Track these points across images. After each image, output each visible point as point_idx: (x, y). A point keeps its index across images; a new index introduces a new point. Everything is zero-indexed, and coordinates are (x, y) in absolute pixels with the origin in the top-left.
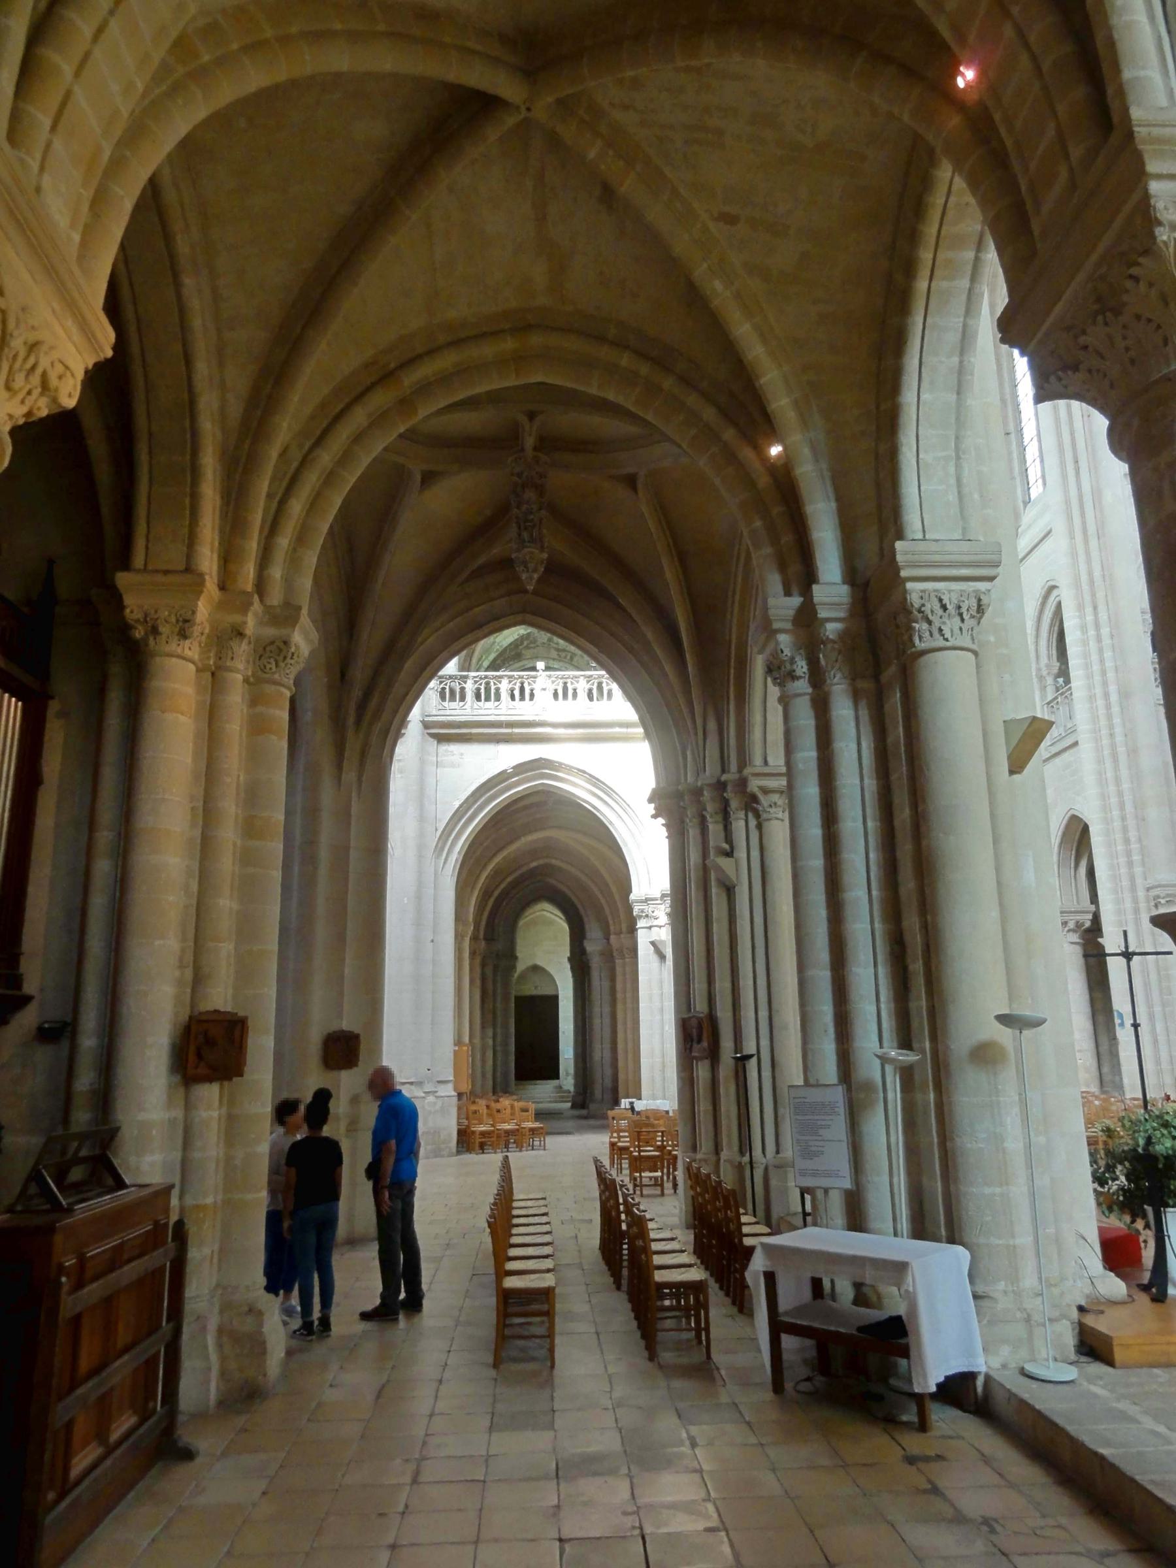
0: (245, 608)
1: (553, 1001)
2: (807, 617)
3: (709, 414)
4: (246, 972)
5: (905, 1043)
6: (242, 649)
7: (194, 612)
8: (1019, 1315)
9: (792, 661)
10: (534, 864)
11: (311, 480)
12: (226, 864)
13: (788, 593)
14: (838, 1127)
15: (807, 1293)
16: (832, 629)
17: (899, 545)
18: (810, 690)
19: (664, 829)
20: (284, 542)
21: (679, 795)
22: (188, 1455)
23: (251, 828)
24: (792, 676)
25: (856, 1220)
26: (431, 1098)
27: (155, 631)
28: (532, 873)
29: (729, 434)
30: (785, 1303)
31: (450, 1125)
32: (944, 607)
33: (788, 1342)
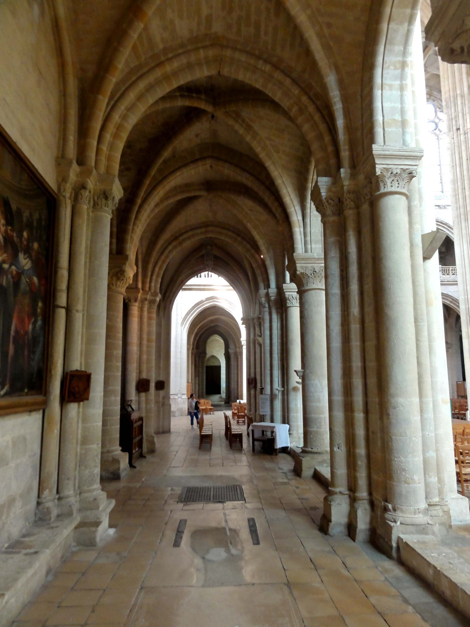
0: (147, 294)
1: (219, 368)
2: (267, 295)
3: (248, 246)
4: (149, 370)
5: (283, 387)
6: (147, 303)
7: (138, 297)
8: (297, 437)
9: (265, 303)
10: (212, 325)
11: (160, 263)
12: (145, 348)
13: (265, 289)
14: (268, 403)
15: (261, 435)
16: (273, 298)
17: (284, 285)
18: (268, 310)
19: (245, 328)
20: (154, 277)
21: (248, 320)
22: (145, 457)
23: (149, 341)
24: (264, 307)
25: (272, 421)
26: (180, 399)
27: (130, 301)
28: (213, 327)
29: (253, 251)
30: (256, 436)
31: (185, 407)
32: (293, 298)
33: (256, 443)
